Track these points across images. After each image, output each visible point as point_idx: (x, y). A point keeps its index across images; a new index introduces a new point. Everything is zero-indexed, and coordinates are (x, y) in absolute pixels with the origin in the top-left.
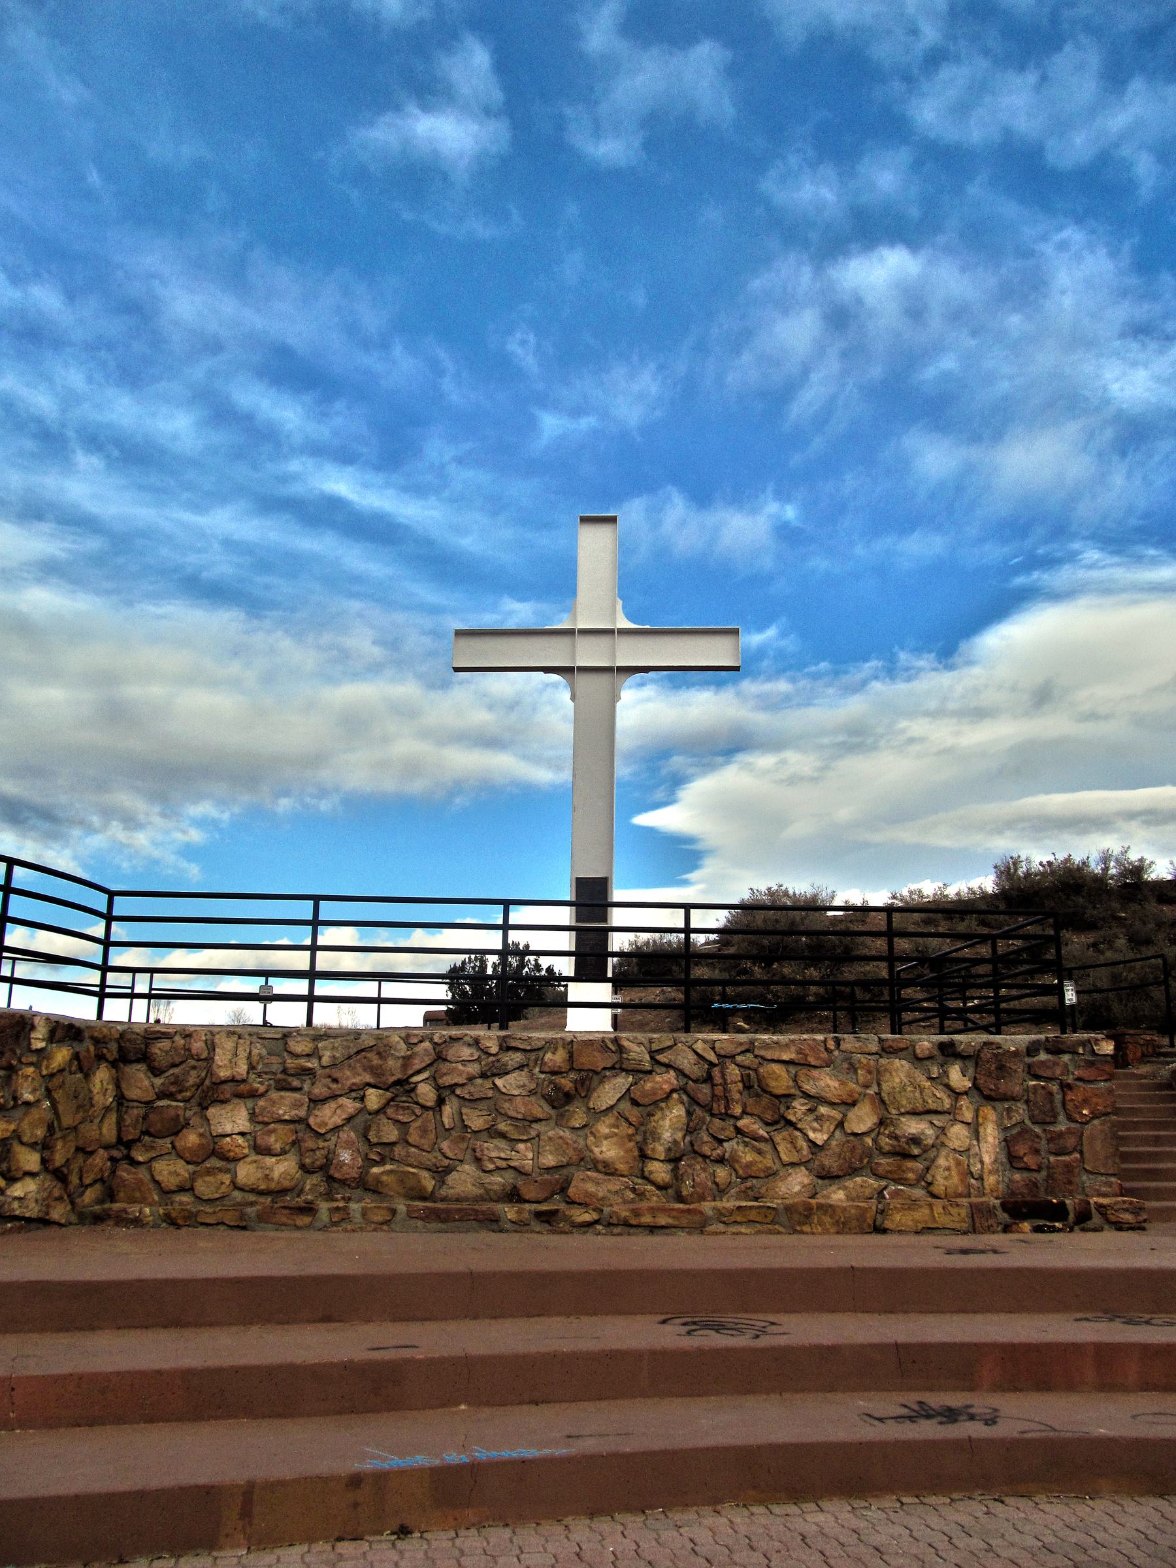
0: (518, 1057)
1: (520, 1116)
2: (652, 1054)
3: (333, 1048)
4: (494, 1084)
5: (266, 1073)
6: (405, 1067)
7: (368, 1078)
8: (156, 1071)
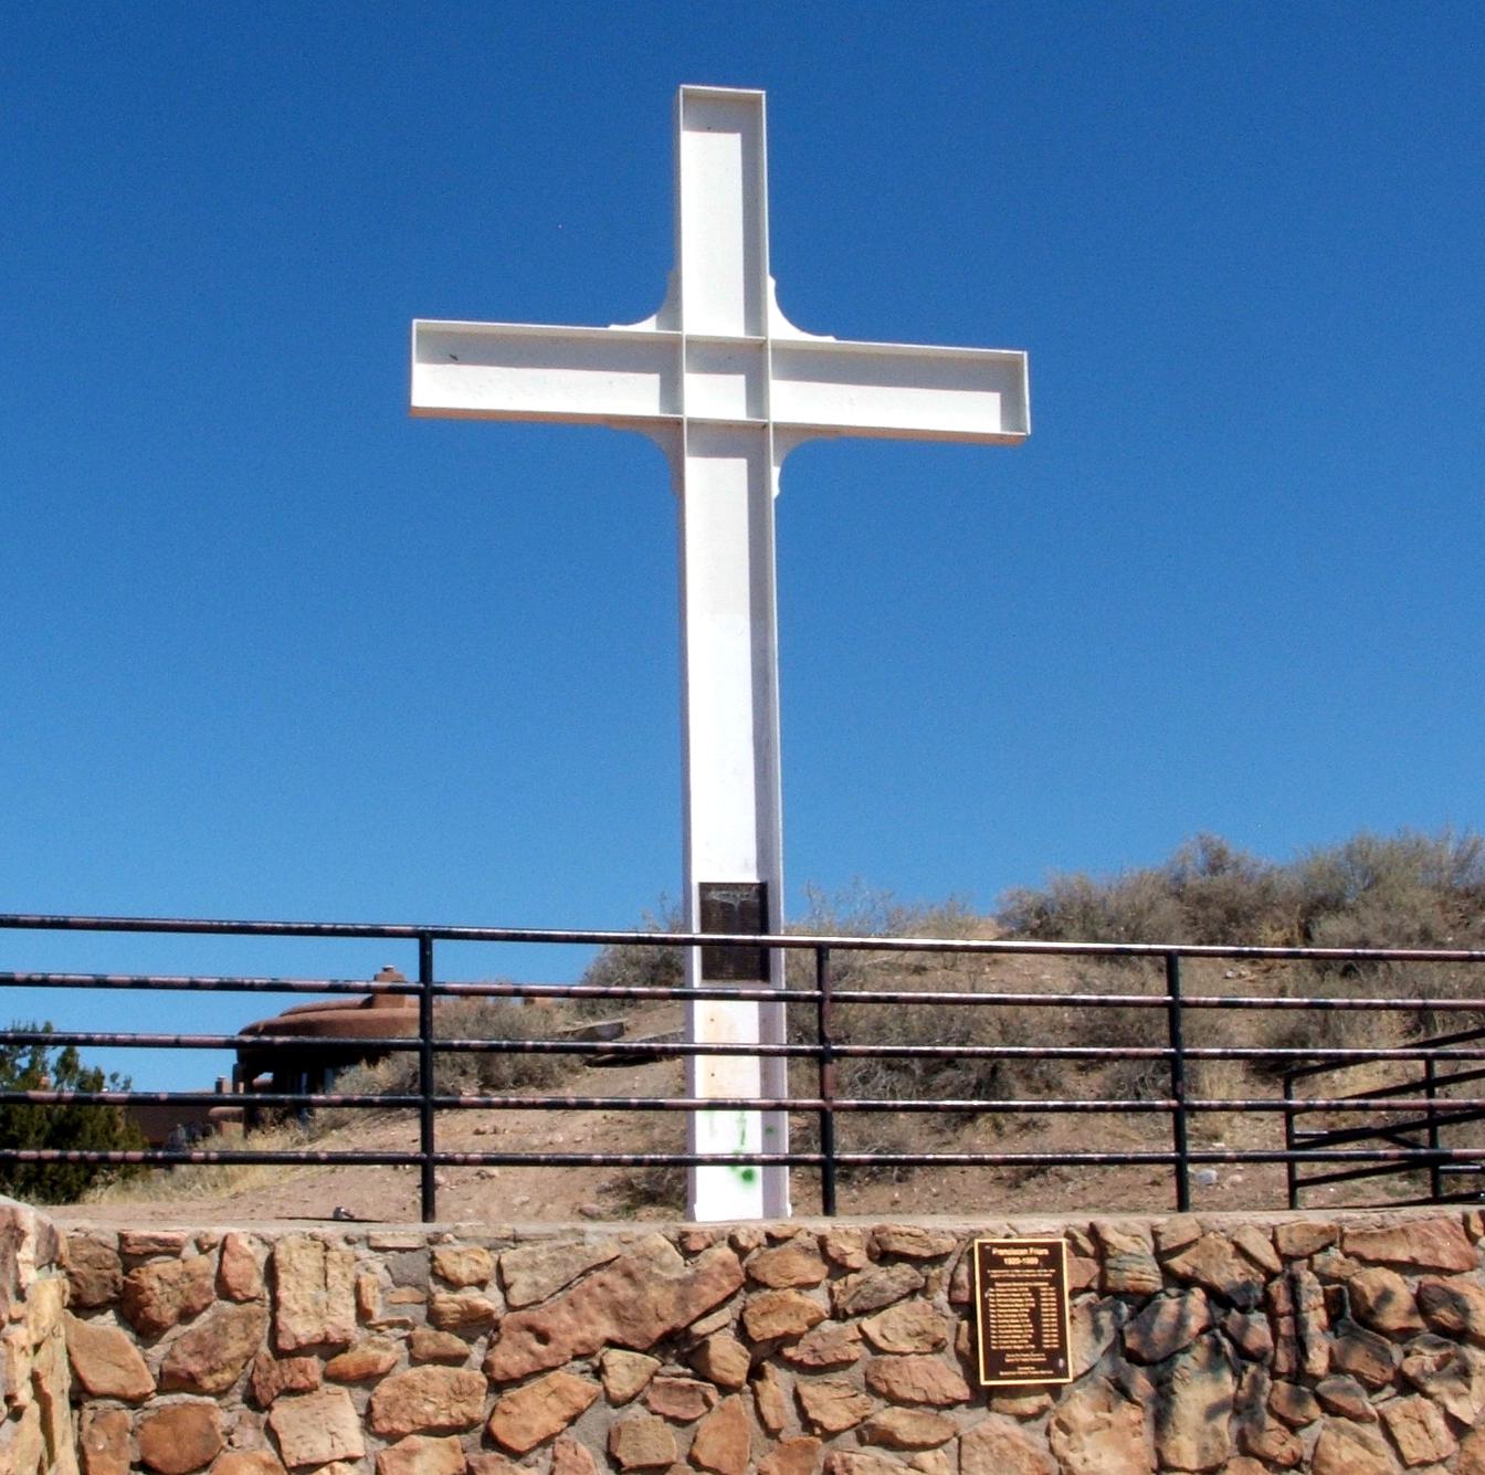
0: (903, 1271)
1: (918, 1397)
2: (1161, 1255)
3: (534, 1267)
4: (860, 1330)
5: (391, 1325)
6: (682, 1300)
7: (607, 1329)
8: (146, 1331)
